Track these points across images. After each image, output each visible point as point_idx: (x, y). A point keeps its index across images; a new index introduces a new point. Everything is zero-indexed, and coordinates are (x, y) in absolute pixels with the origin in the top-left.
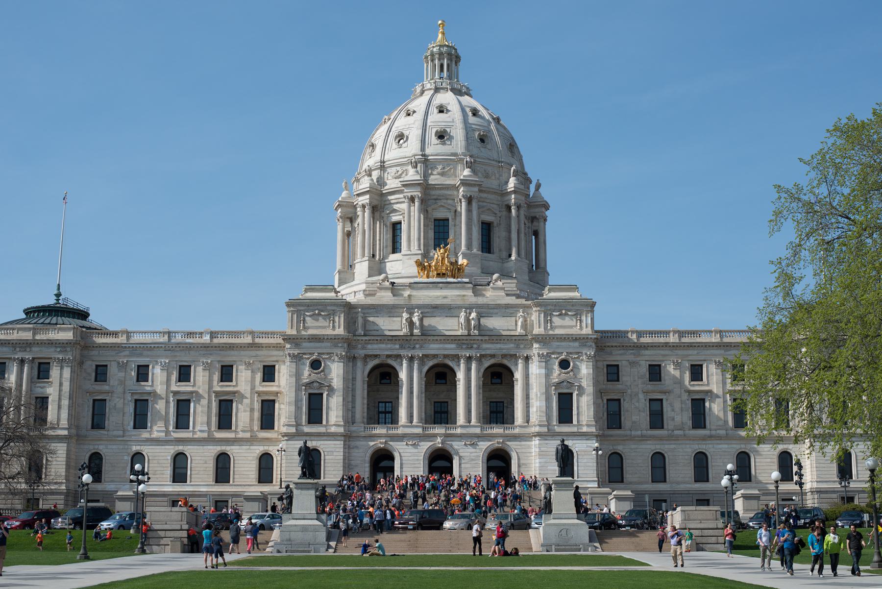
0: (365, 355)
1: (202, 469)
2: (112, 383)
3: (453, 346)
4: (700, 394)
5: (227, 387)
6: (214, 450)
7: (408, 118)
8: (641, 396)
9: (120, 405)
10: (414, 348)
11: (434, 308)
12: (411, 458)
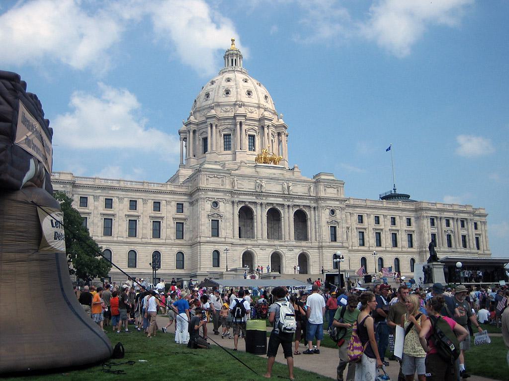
0: (239, 201)
1: (144, 260)
2: (90, 208)
3: (281, 199)
5: (158, 214)
6: (151, 249)
7: (229, 83)
8: (355, 230)
9: (95, 221)
10: (262, 199)
11: (271, 179)
12: (263, 257)
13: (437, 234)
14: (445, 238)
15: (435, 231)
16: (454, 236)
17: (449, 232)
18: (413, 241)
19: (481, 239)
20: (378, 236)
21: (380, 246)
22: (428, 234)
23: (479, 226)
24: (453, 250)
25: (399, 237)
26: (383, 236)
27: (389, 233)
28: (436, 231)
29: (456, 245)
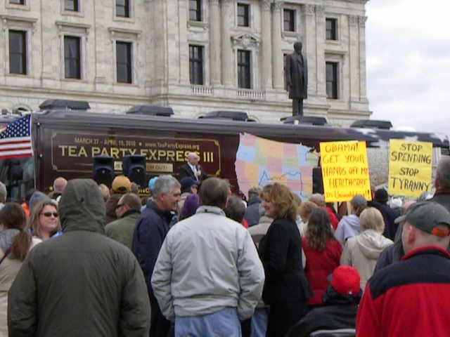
4: (20, 24)
13: (206, 46)
14: (233, 59)
15: (200, 37)
16: (260, 54)
17: (246, 41)
18: (135, 65)
19: (344, 70)
20: (73, 46)
21: (25, 72)
22: (179, 45)
23: (342, 31)
24: (253, 97)
25: (87, 49)
26: (33, 42)
27: (55, 33)
28: (205, 37)
29: (263, 82)
